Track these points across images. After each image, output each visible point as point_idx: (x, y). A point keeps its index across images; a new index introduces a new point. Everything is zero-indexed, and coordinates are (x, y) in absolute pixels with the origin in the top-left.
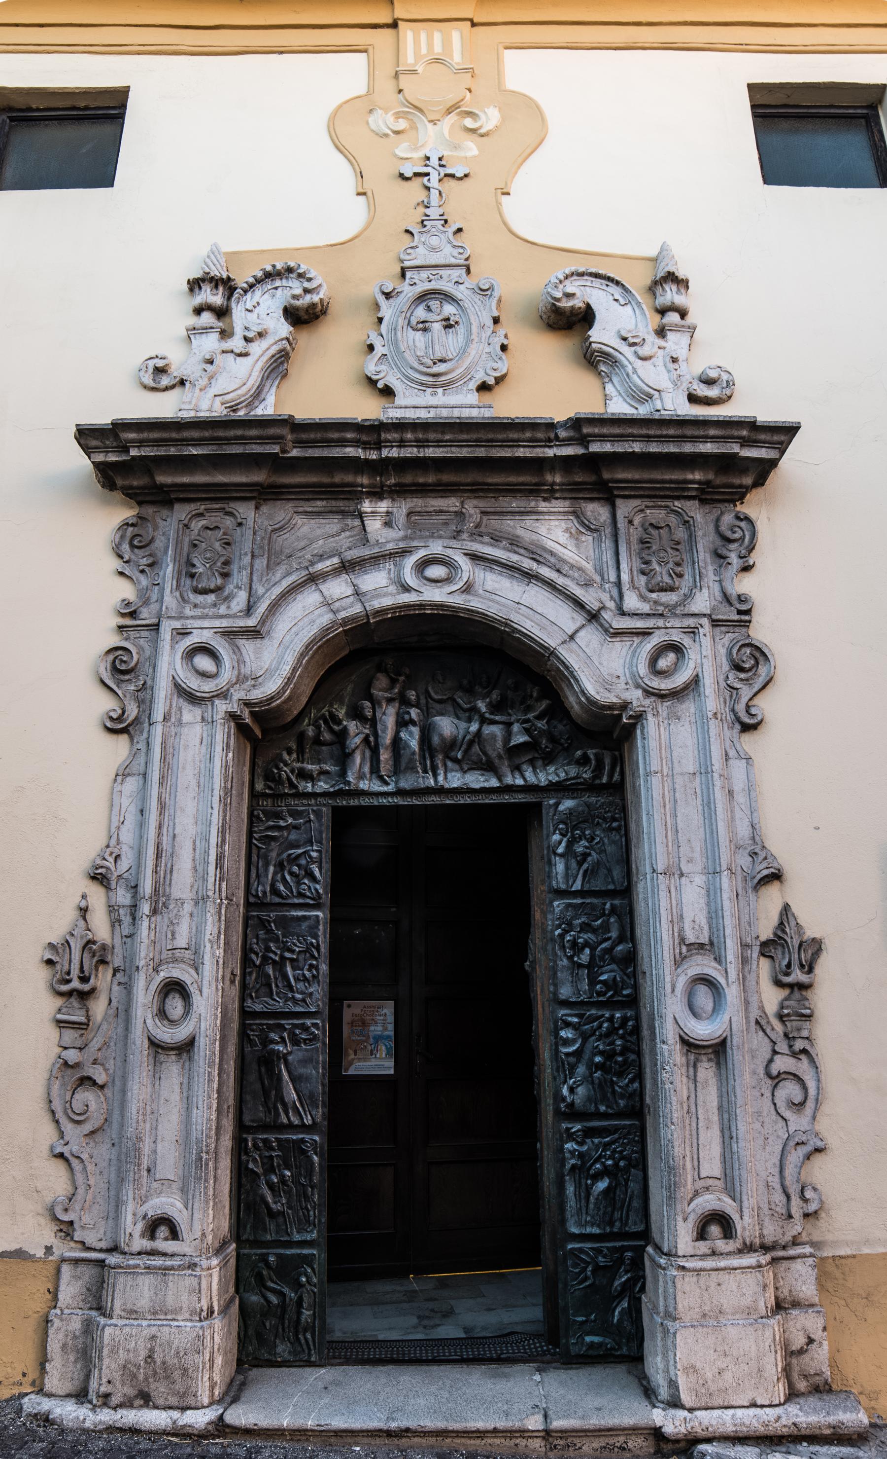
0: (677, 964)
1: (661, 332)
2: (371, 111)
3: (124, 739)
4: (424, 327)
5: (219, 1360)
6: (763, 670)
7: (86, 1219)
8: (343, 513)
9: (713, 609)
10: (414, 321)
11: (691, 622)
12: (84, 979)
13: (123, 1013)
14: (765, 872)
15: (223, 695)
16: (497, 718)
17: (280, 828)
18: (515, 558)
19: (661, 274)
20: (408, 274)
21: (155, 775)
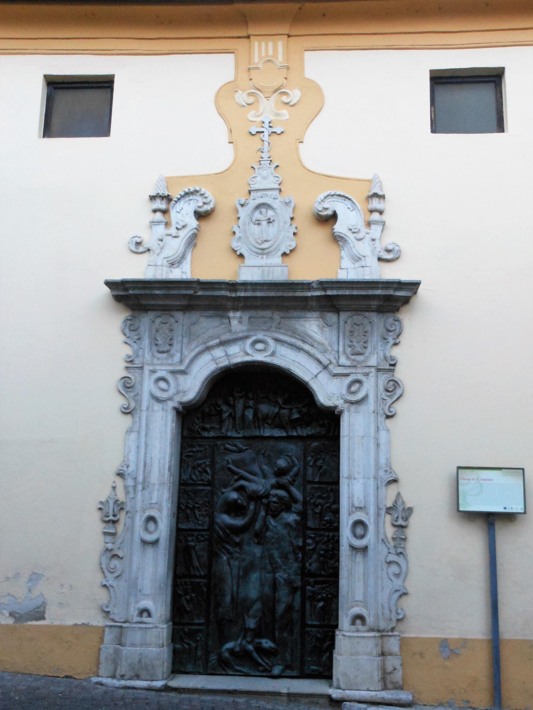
0: (350, 514)
1: (369, 224)
2: (236, 91)
3: (129, 417)
4: (258, 223)
5: (166, 664)
6: (398, 392)
7: (116, 611)
8: (222, 317)
9: (378, 364)
10: (254, 219)
11: (367, 370)
12: (114, 516)
13: (130, 529)
14: (390, 479)
15: (170, 399)
16: (286, 406)
17: (193, 452)
18: (293, 341)
19: (371, 193)
20: (252, 193)
21: (143, 433)
